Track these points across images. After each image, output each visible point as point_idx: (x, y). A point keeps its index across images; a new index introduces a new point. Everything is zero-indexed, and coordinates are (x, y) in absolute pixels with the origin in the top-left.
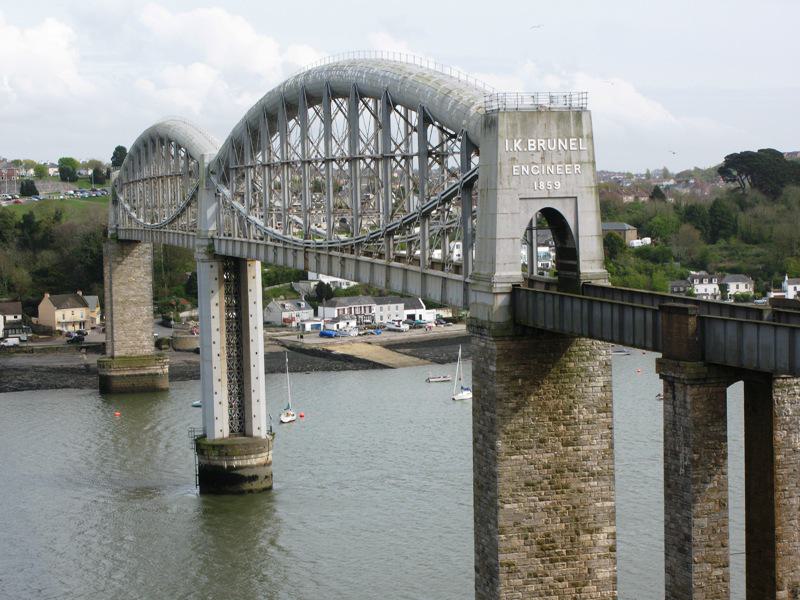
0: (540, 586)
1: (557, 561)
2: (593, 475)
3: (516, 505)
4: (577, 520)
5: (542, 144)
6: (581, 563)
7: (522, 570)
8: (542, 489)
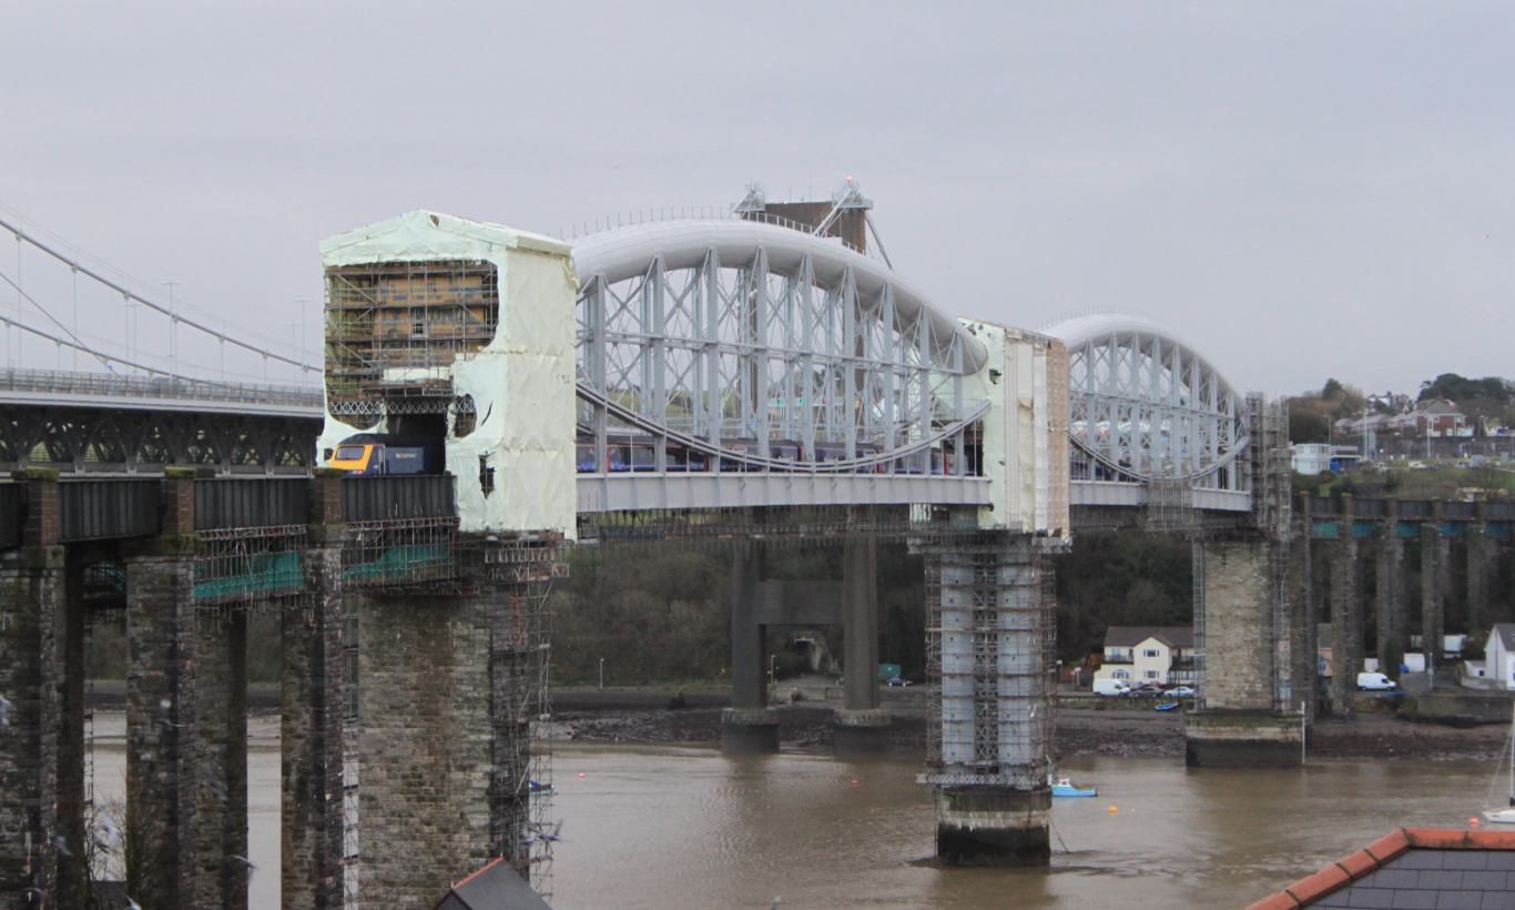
0: (404, 828)
1: (420, 799)
2: (467, 700)
3: (378, 730)
6: (451, 805)
7: (384, 807)
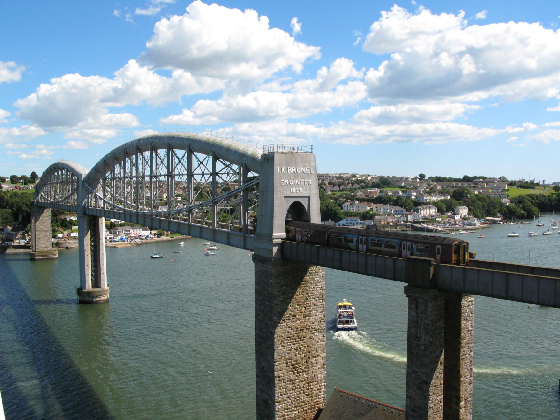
1: (300, 372)
4: (309, 352)
8: (294, 339)
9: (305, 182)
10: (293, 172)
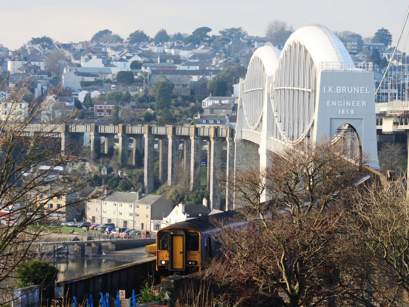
5: (344, 89)
9: (358, 104)
10: (343, 92)
